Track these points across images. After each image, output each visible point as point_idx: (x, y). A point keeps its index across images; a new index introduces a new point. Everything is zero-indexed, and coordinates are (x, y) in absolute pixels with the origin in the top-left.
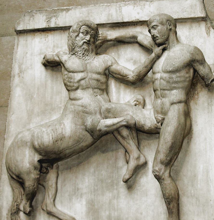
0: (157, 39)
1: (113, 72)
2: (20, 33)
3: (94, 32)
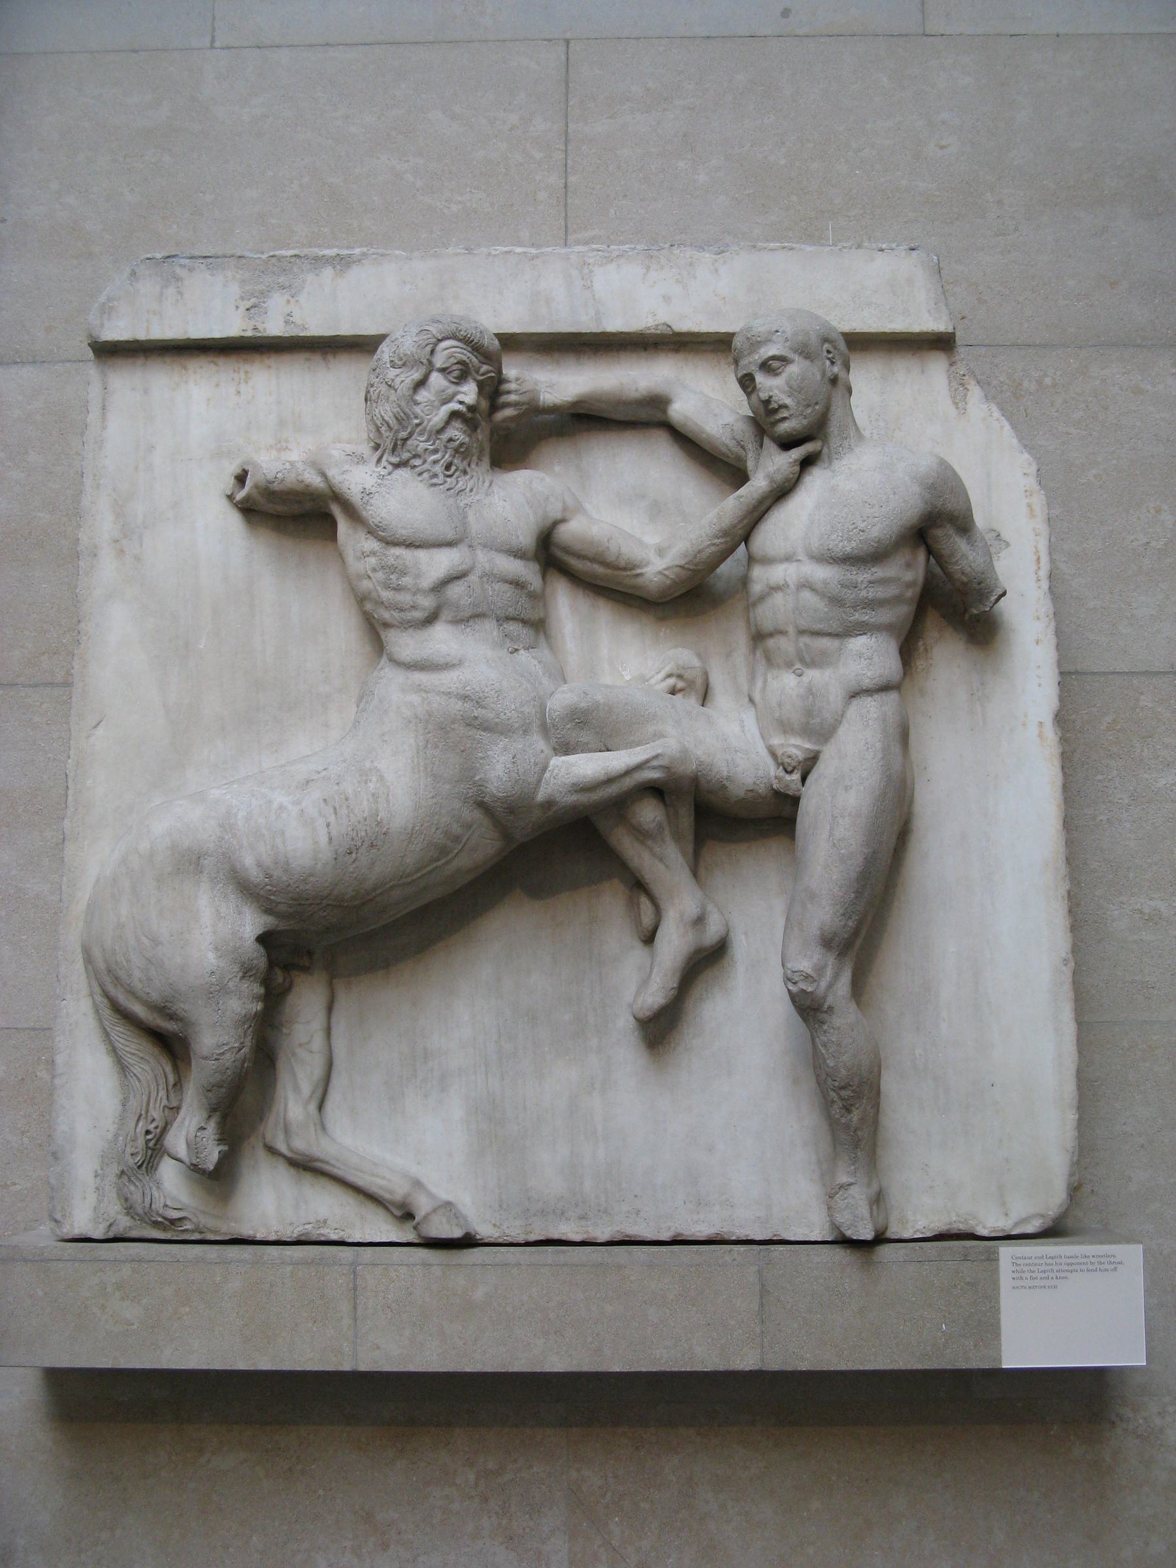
0: (784, 419)
1: (567, 550)
2: (110, 352)
3: (491, 368)
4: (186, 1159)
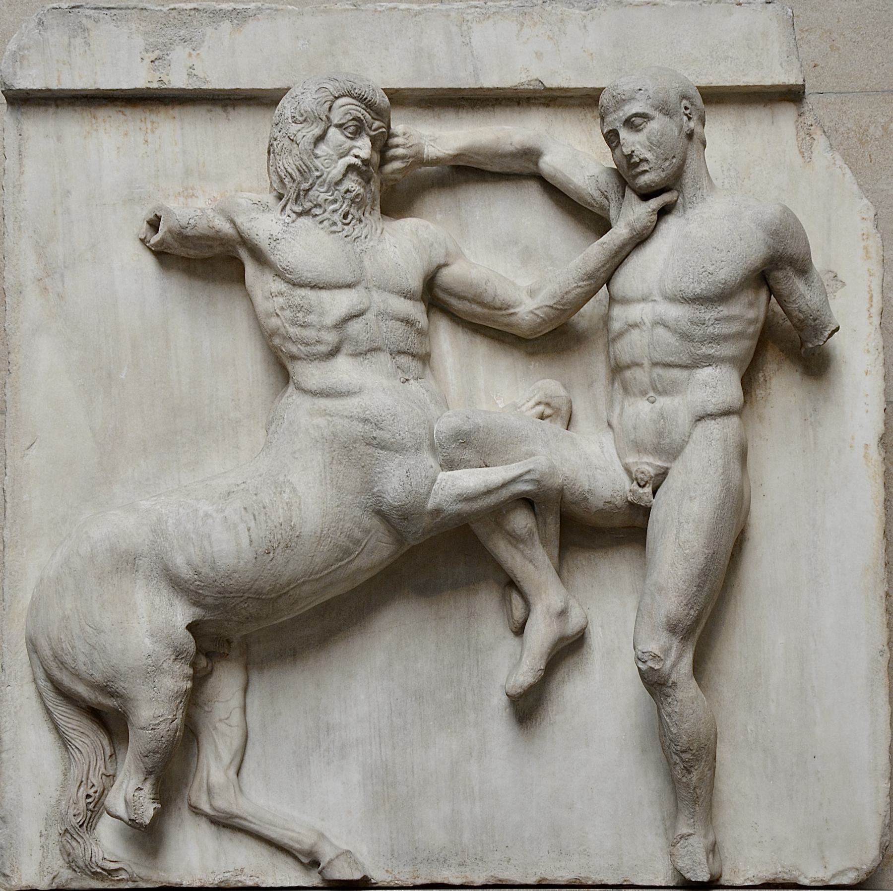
3: (382, 124)
4: (125, 816)
